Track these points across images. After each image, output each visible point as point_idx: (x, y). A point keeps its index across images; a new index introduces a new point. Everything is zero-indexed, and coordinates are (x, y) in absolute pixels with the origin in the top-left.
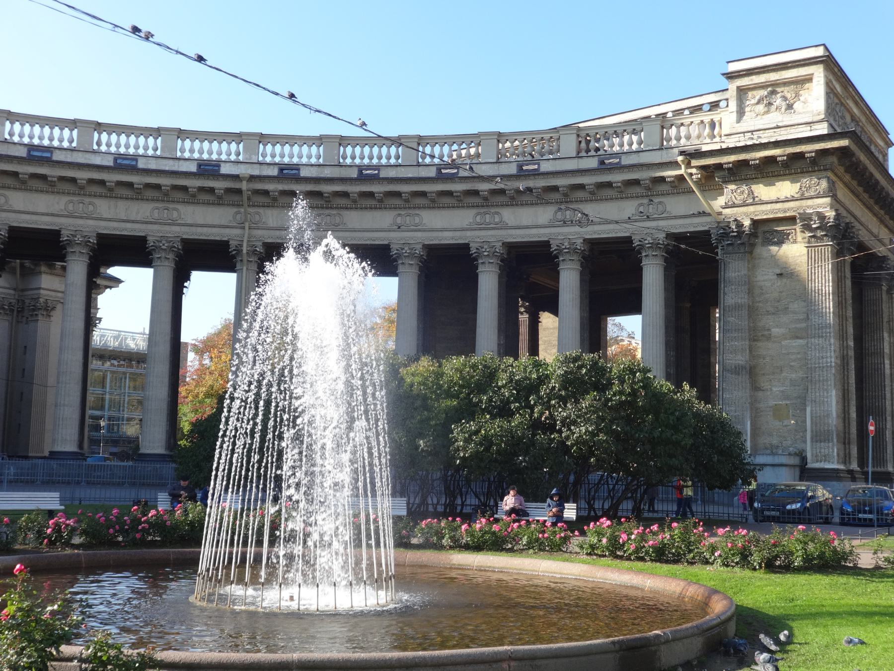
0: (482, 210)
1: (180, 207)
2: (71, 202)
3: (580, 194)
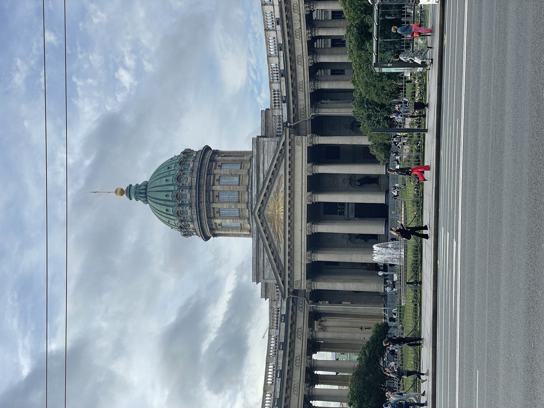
2: (296, 37)
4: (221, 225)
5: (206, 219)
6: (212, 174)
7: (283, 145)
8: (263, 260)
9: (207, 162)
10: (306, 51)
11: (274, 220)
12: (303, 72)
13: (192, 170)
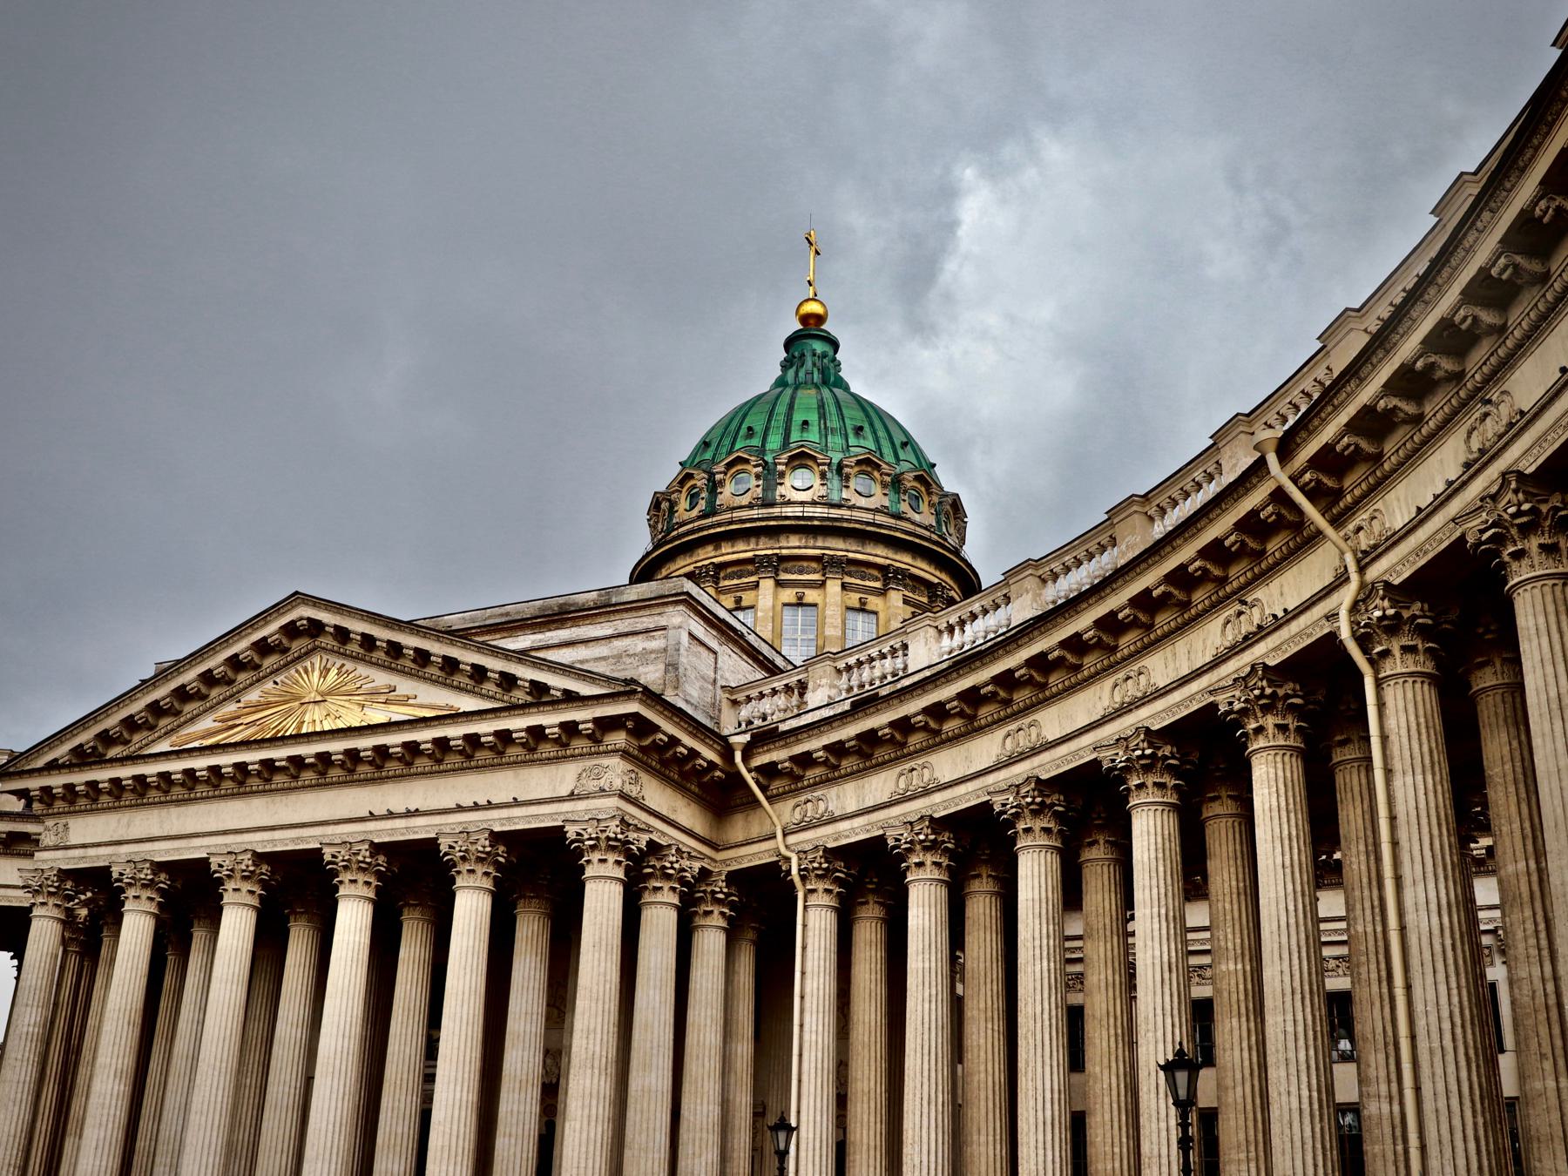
6: (824, 575)
7: (566, 692)
9: (876, 556)
10: (1058, 766)
11: (286, 702)
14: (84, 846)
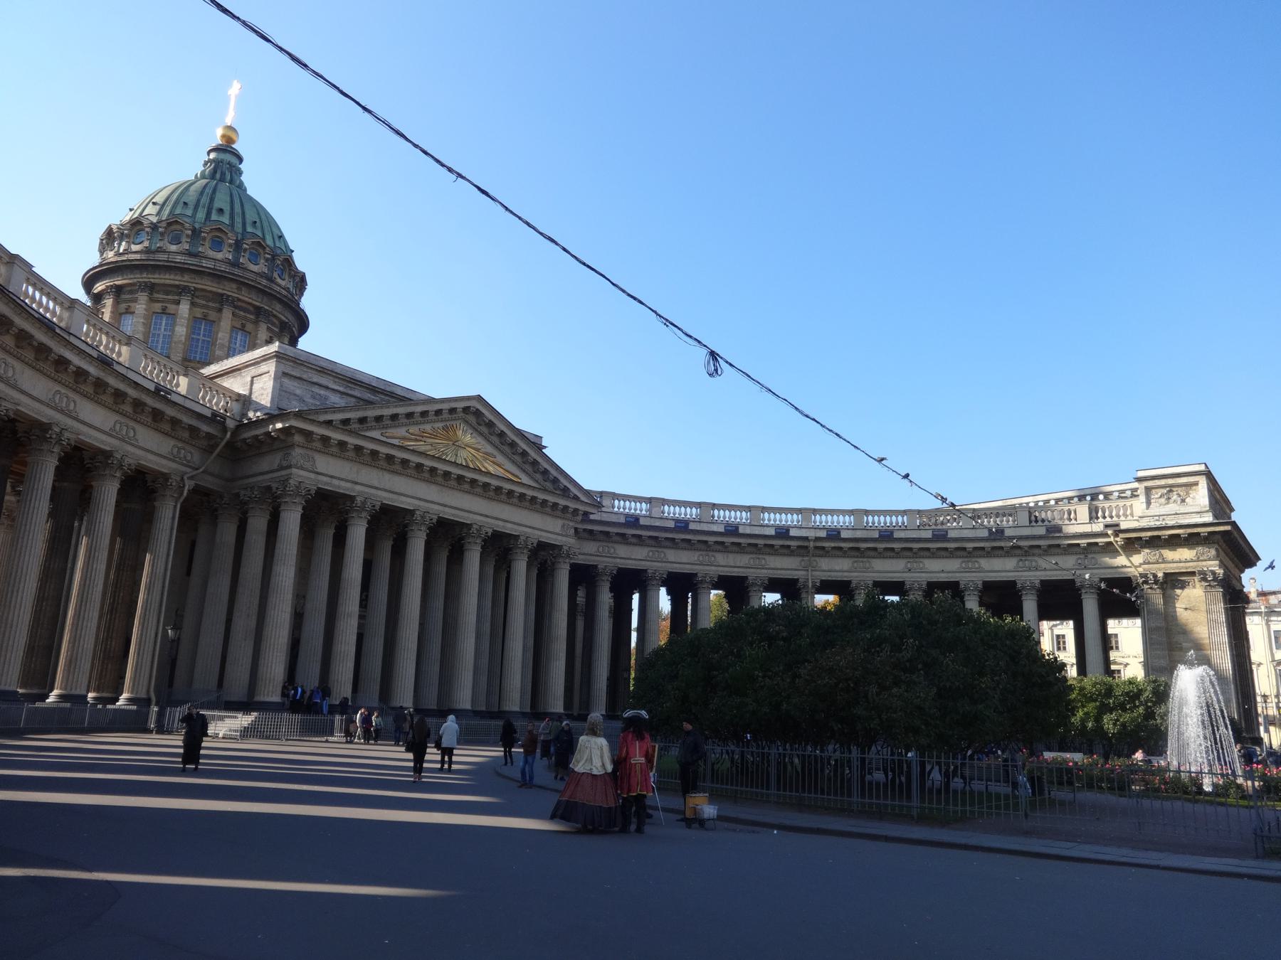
0: (966, 560)
1: (767, 557)
2: (702, 555)
3: (1036, 551)
4: (163, 313)
5: (194, 285)
8: (327, 388)
11: (446, 440)
12: (633, 557)
13: (292, 295)
14: (332, 477)
